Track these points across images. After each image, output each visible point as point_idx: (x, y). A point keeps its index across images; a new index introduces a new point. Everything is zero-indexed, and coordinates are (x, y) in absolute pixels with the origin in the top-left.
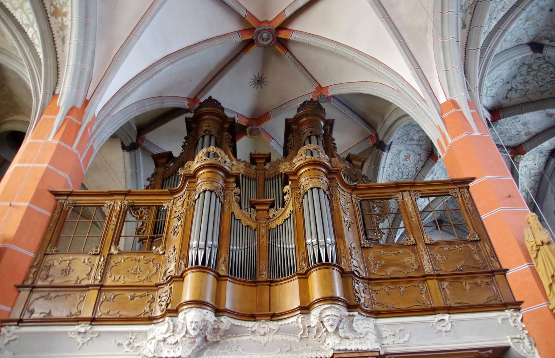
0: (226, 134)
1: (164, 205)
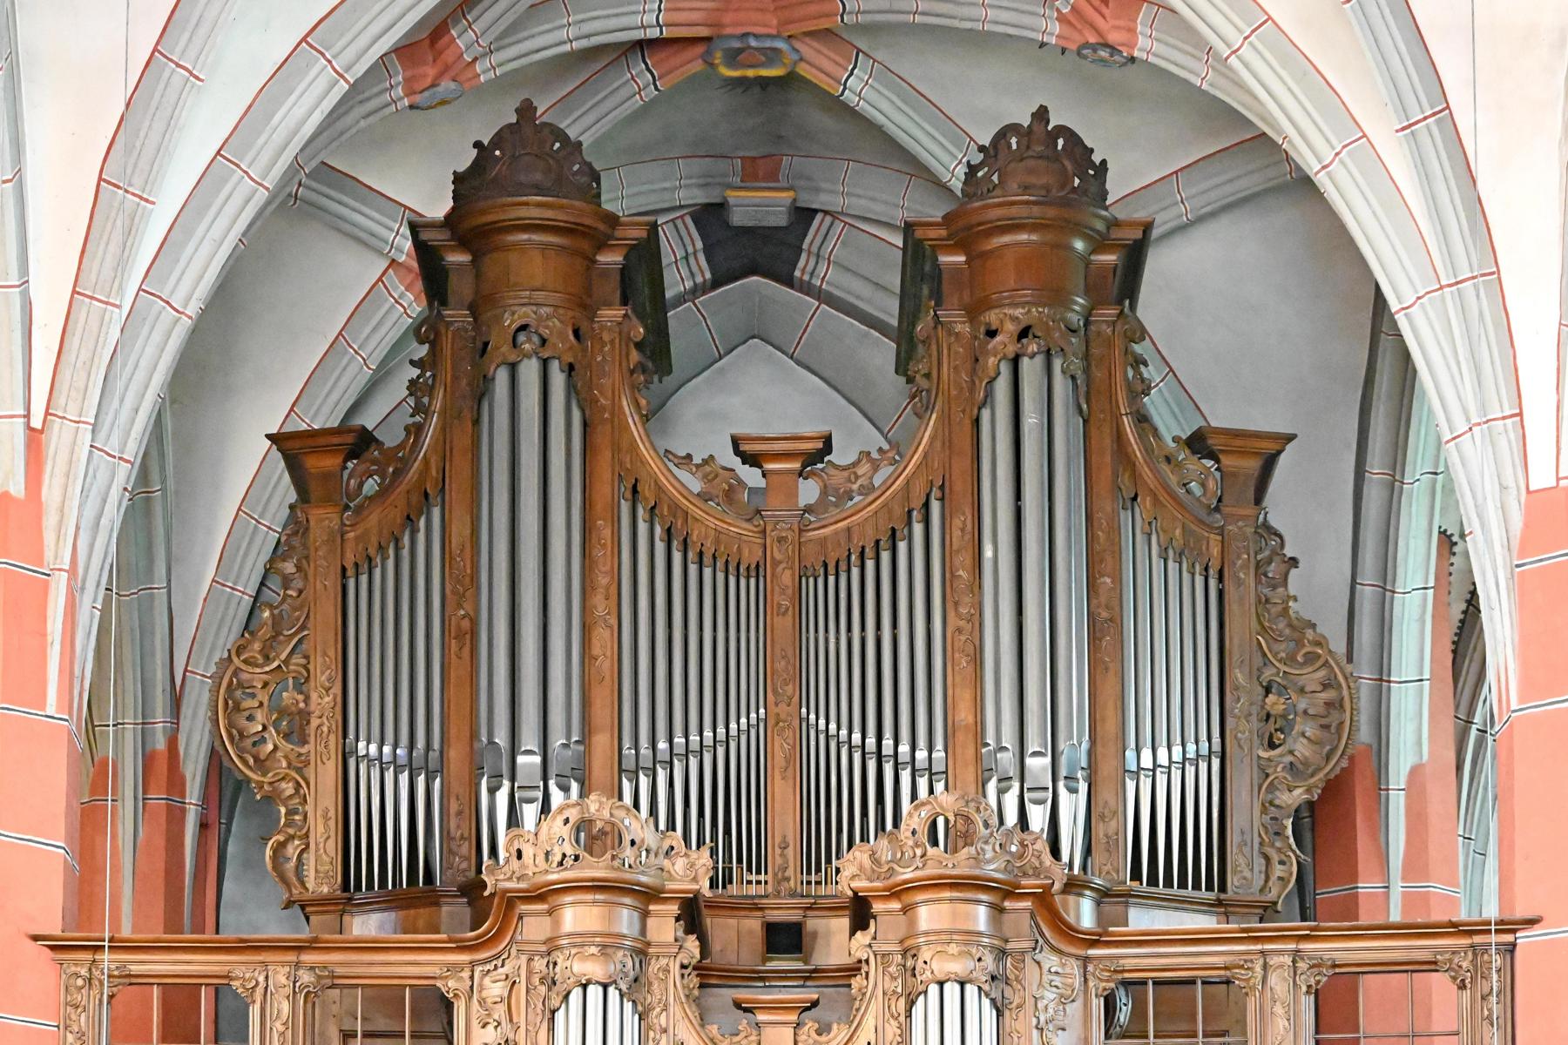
0: (611, 314)
1: (439, 984)
